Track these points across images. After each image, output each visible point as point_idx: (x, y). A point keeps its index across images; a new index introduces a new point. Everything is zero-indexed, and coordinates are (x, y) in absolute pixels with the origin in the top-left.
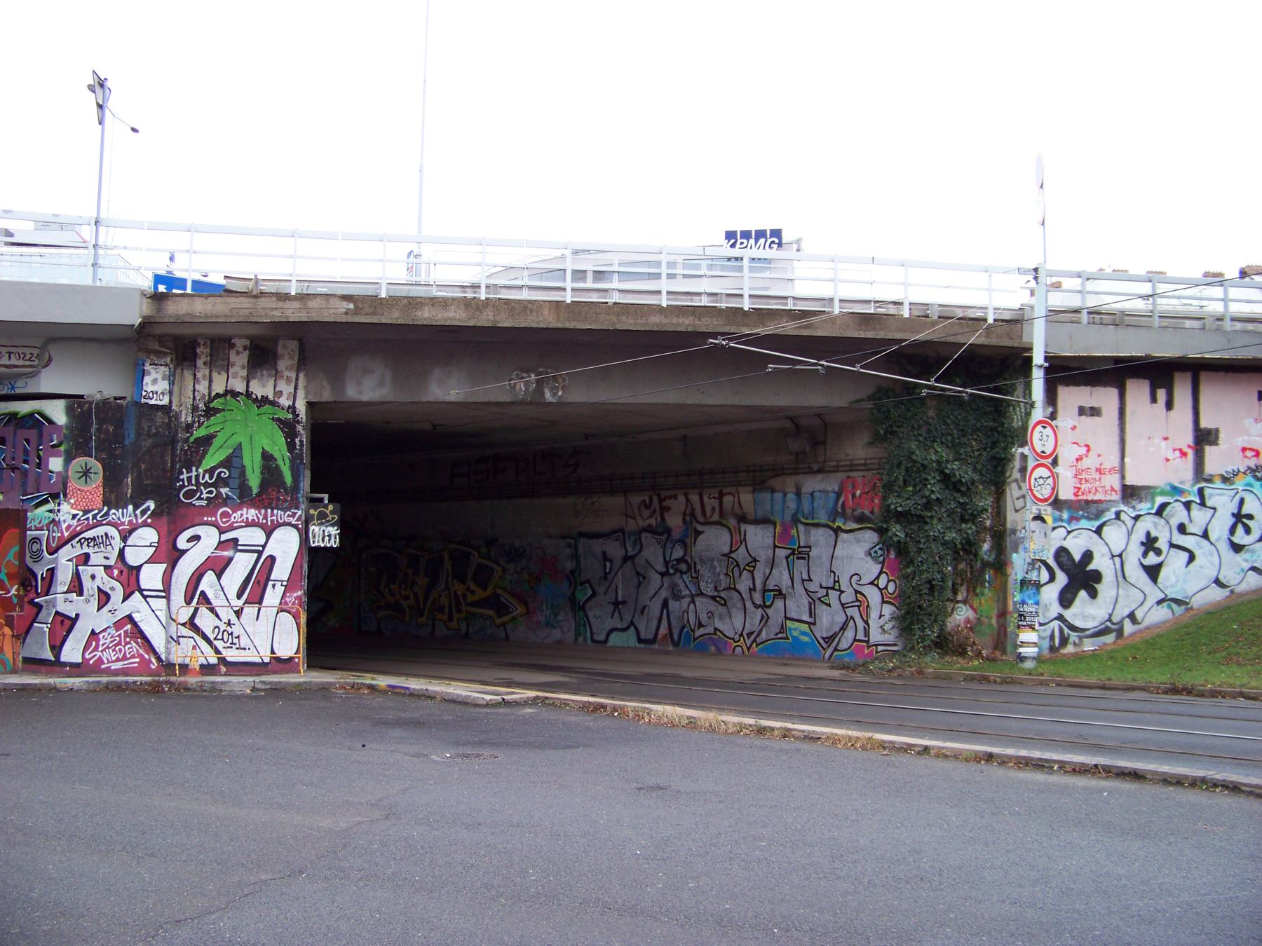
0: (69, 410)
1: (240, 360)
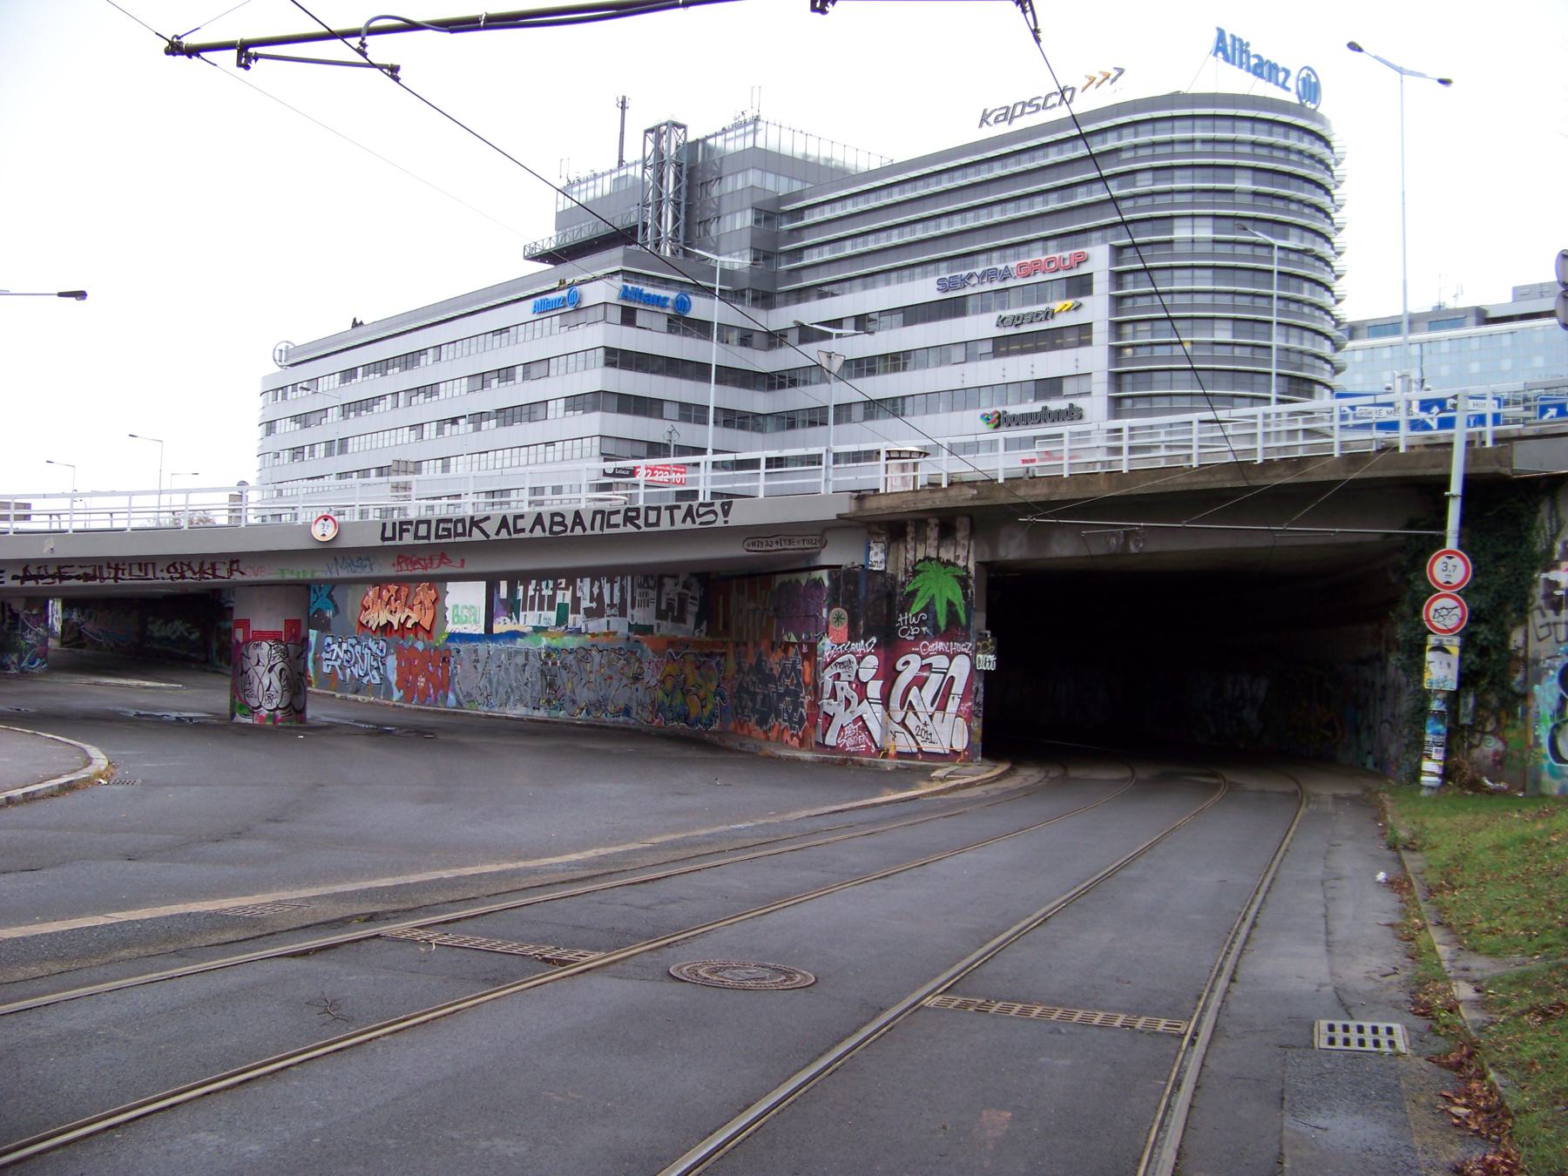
0: (830, 576)
1: (933, 534)
